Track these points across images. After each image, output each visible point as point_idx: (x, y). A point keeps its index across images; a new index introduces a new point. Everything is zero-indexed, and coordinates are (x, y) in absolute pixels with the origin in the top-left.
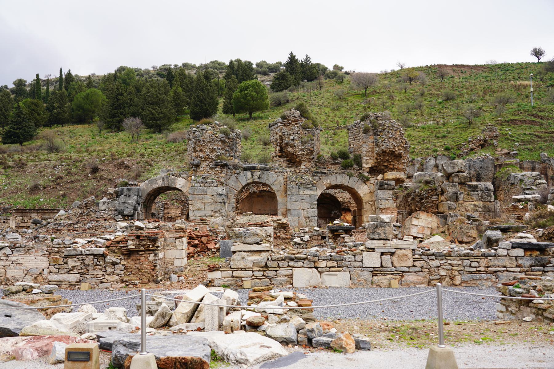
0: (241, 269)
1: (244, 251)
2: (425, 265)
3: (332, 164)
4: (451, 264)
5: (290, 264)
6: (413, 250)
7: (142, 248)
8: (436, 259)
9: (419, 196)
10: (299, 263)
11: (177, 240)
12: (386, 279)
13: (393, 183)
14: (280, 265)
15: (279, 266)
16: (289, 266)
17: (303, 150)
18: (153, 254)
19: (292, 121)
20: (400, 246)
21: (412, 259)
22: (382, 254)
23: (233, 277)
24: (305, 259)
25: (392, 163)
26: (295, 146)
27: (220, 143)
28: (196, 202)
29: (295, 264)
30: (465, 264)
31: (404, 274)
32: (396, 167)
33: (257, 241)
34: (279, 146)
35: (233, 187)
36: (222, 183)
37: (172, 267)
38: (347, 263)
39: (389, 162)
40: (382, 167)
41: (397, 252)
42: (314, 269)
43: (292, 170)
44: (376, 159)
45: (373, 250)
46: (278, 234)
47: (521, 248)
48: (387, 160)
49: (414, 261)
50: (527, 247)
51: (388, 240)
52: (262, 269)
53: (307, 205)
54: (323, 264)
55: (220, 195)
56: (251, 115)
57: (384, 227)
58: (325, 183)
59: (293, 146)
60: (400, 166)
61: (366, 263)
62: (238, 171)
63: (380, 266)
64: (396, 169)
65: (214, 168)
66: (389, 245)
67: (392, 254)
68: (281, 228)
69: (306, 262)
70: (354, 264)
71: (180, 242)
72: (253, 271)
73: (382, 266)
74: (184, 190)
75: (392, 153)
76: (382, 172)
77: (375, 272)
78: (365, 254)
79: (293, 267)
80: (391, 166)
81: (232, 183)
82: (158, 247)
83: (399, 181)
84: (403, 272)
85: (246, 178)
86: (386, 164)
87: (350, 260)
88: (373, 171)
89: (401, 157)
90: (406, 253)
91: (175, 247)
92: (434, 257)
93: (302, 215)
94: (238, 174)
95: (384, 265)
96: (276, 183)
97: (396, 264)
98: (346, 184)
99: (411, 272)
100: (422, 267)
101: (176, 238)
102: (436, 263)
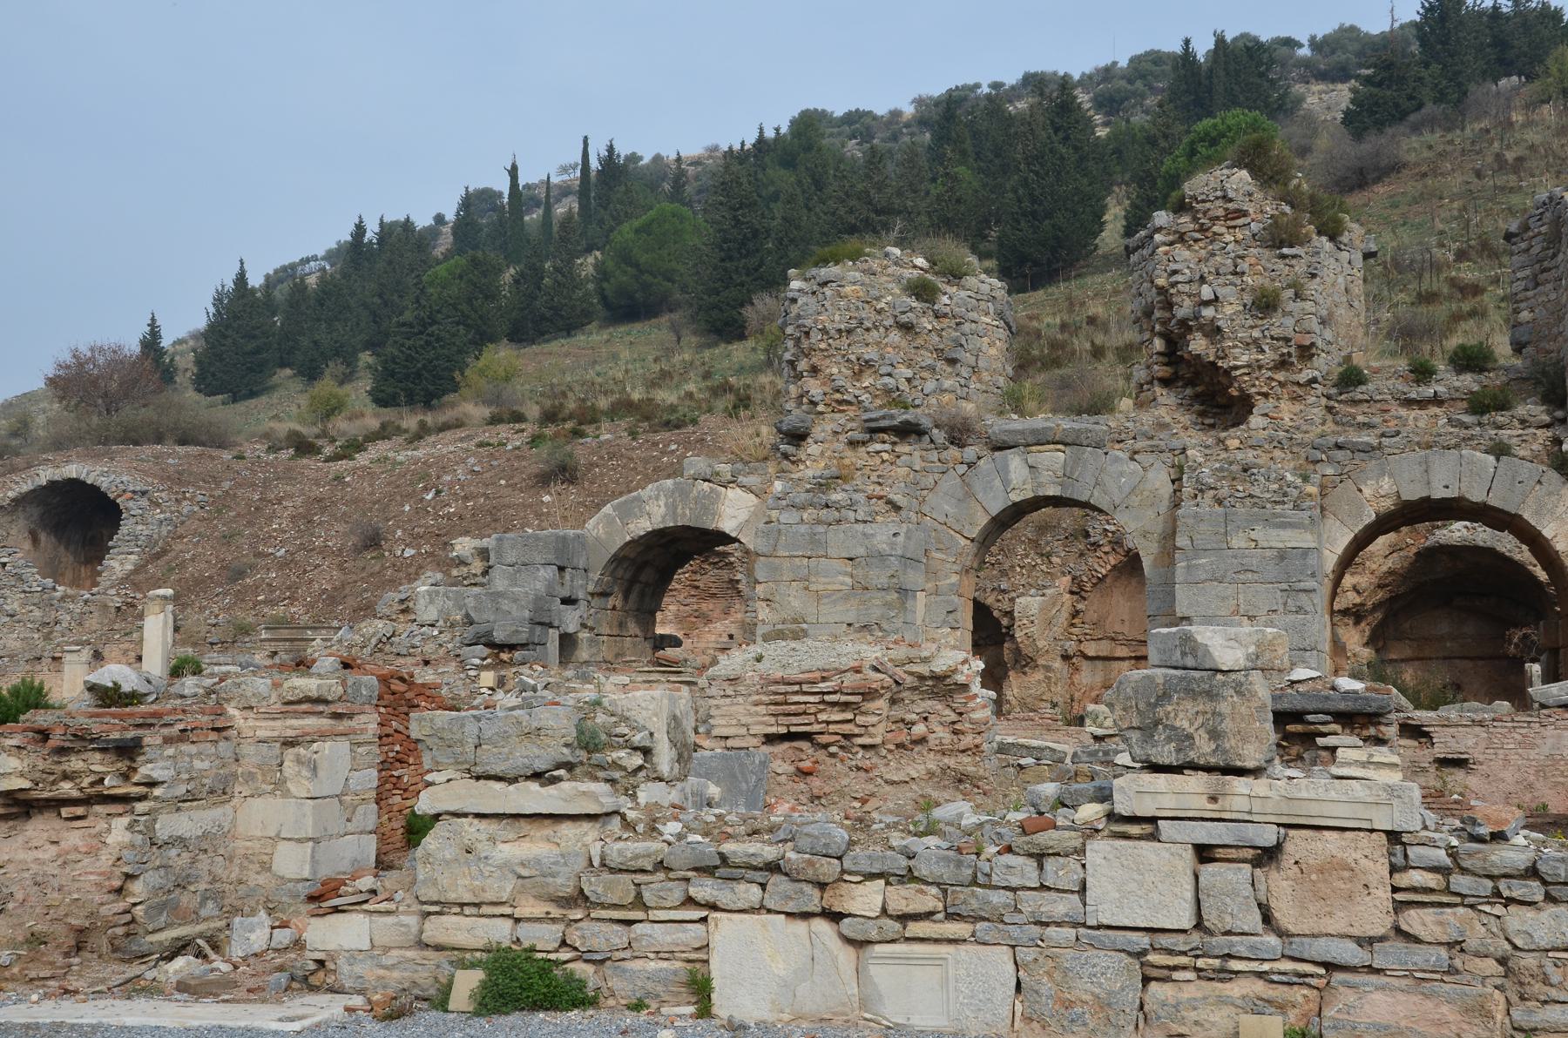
0: (462, 905)
2: (1476, 933)
3: (1408, 403)
5: (692, 891)
6: (1394, 836)
7: (67, 789)
8: (1550, 899)
10: (741, 887)
11: (290, 753)
12: (1222, 1001)
14: (647, 895)
15: (639, 902)
16: (690, 901)
17: (1256, 344)
18: (125, 820)
20: (1314, 809)
21: (1383, 895)
22: (1204, 853)
23: (423, 945)
24: (773, 867)
26: (1219, 329)
27: (895, 336)
28: (783, 588)
31: (1339, 976)
33: (540, 765)
34: (1161, 335)
35: (950, 521)
37: (261, 879)
38: (998, 898)
41: (1289, 847)
42: (822, 926)
45: (1150, 825)
46: (919, 729)
49: (1399, 907)
51: (1241, 772)
52: (556, 912)
54: (865, 899)
55: (882, 556)
57: (1211, 695)
58: (1367, 492)
59: (1213, 332)
61: (1106, 905)
62: (970, 452)
63: (1187, 921)
67: (1268, 856)
68: (934, 695)
69: (777, 882)
70: (1031, 903)
71: (299, 760)
73: (1199, 925)
78: (1099, 850)
79: (714, 907)
81: (943, 504)
84: (1330, 966)
85: (1006, 482)
87: (1015, 881)
90: (1350, 856)
91: (280, 786)
92: (1535, 890)
94: (970, 465)
95: (1211, 919)
96: (1135, 500)
97: (1285, 915)
99: (1378, 971)
100: (1455, 945)
101: (289, 743)
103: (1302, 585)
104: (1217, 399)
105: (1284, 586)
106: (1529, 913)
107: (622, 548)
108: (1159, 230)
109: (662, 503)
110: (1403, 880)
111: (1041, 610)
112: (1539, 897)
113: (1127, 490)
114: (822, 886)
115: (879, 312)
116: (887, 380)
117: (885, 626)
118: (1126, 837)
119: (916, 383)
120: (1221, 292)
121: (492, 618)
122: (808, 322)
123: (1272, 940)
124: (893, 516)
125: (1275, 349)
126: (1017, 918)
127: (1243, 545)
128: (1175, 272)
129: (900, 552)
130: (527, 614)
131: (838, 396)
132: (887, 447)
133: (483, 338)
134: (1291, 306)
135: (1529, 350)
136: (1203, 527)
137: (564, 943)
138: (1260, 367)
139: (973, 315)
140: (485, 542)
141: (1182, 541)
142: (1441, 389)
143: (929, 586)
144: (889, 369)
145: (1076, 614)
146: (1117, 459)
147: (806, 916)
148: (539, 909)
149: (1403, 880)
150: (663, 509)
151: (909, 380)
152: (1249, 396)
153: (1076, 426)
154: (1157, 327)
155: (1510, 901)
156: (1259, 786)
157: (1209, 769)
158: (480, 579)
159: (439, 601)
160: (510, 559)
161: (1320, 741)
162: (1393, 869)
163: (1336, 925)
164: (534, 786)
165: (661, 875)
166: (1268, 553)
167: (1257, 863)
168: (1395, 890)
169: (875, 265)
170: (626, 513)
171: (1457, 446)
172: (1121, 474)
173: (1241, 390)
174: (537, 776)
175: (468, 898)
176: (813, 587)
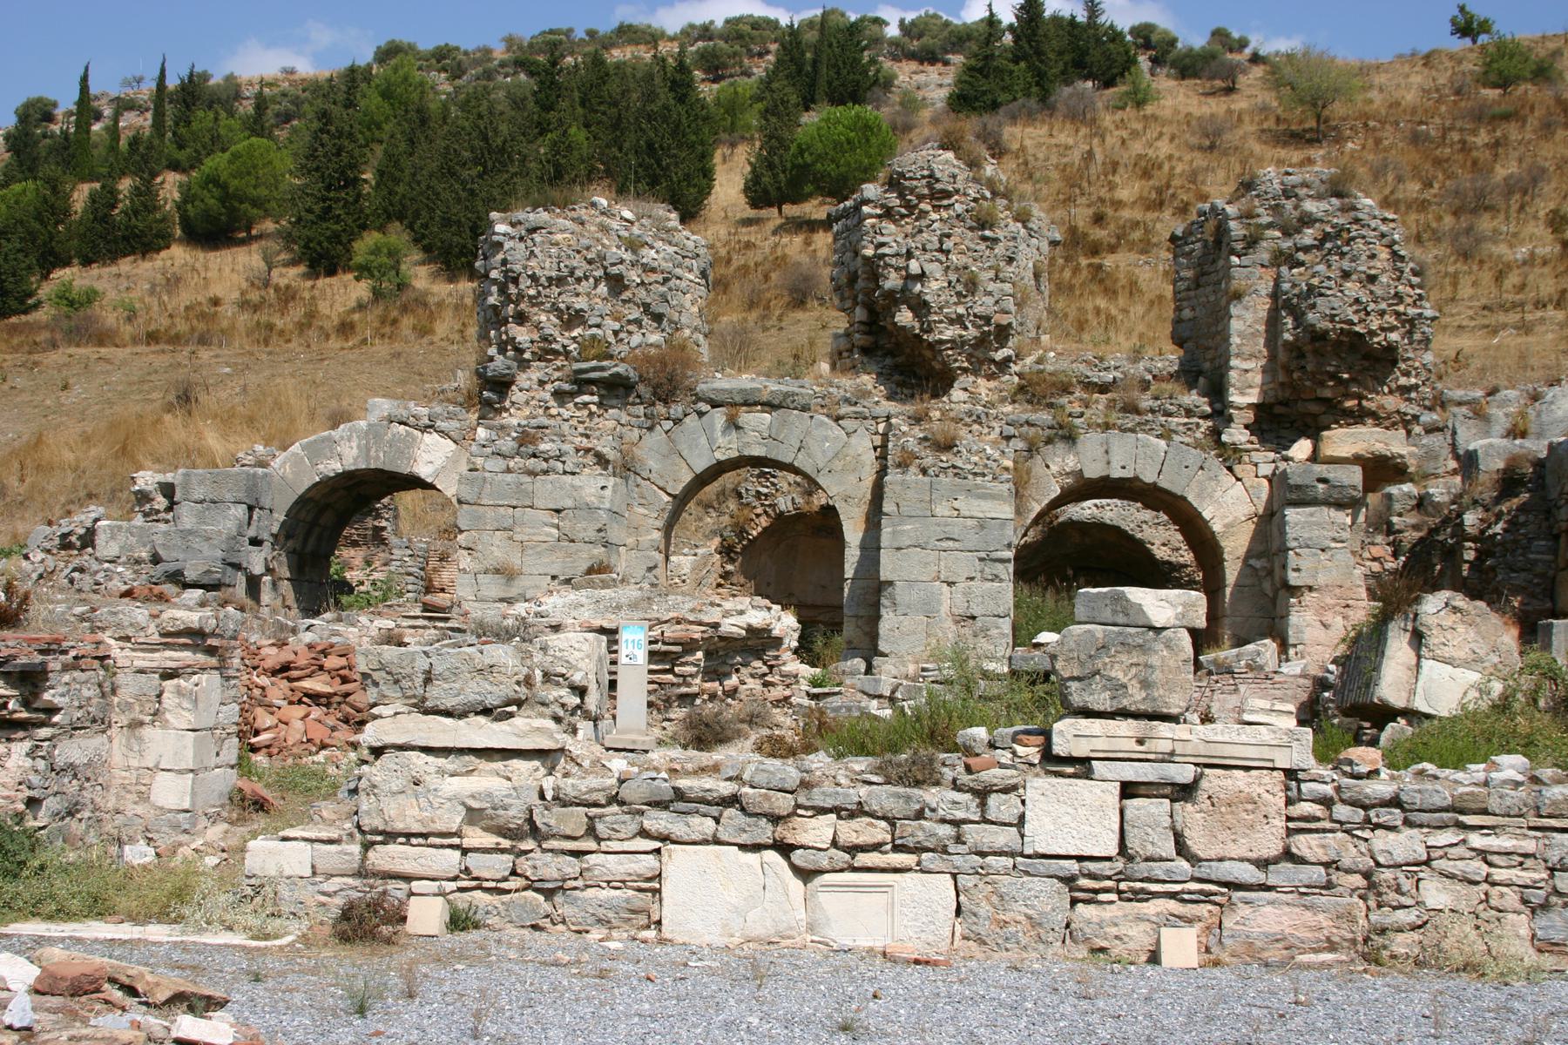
0: (409, 836)
1: (427, 750)
2: (1351, 854)
4: (1483, 854)
5: (647, 824)
6: (1290, 774)
8: (1408, 823)
10: (695, 820)
12: (1139, 919)
13: (1355, 476)
15: (591, 832)
16: (644, 833)
17: (959, 320)
18: (27, 745)
19: (921, 198)
21: (1280, 823)
22: (1129, 790)
26: (926, 303)
28: (486, 537)
29: (677, 828)
33: (491, 701)
36: (602, 460)
37: (140, 810)
39: (1341, 382)
40: (1314, 408)
41: (1204, 784)
42: (771, 856)
43: (909, 408)
45: (1082, 766)
48: (1333, 376)
49: (1290, 832)
52: (506, 843)
53: (963, 564)
54: (816, 831)
58: (1054, 468)
59: (920, 307)
60: (1391, 402)
63: (1113, 850)
65: (572, 395)
66: (1165, 746)
67: (1184, 792)
71: (179, 692)
72: (465, 852)
74: (450, 488)
76: (1313, 431)
77: (1080, 881)
79: (665, 838)
80: (1349, 404)
82: (52, 710)
83: (1381, 470)
86: (1328, 394)
87: (960, 815)
89: (1394, 362)
92: (1395, 817)
93: (944, 609)
94: (677, 421)
95: (1133, 843)
96: (838, 465)
97: (1196, 844)
98: (1149, 477)
102: (1403, 844)
105: (983, 555)
106: (1392, 836)
107: (309, 490)
108: (867, 202)
109: (354, 444)
111: (693, 569)
112: (1399, 823)
113: (830, 454)
115: (590, 262)
116: (594, 331)
119: (622, 335)
120: (928, 268)
121: (181, 557)
122: (518, 268)
123: (1185, 865)
124: (598, 469)
125: (978, 327)
126: (961, 848)
127: (947, 513)
128: (883, 245)
129: (607, 505)
130: (219, 554)
134: (991, 287)
135: (1189, 345)
136: (910, 494)
137: (514, 873)
139: (678, 271)
140: (169, 477)
141: (888, 507)
144: (599, 320)
146: (822, 424)
147: (757, 848)
148: (490, 840)
150: (355, 451)
151: (616, 333)
152: (951, 370)
153: (784, 388)
154: (860, 297)
155: (1378, 826)
156: (1179, 731)
157: (1136, 716)
158: (162, 516)
159: (122, 537)
160: (198, 496)
162: (1289, 802)
165: (615, 808)
166: (969, 522)
168: (1289, 819)
169: (582, 213)
170: (314, 452)
171: (1132, 430)
172: (826, 439)
173: (944, 363)
174: (486, 712)
175: (416, 828)
176: (517, 537)
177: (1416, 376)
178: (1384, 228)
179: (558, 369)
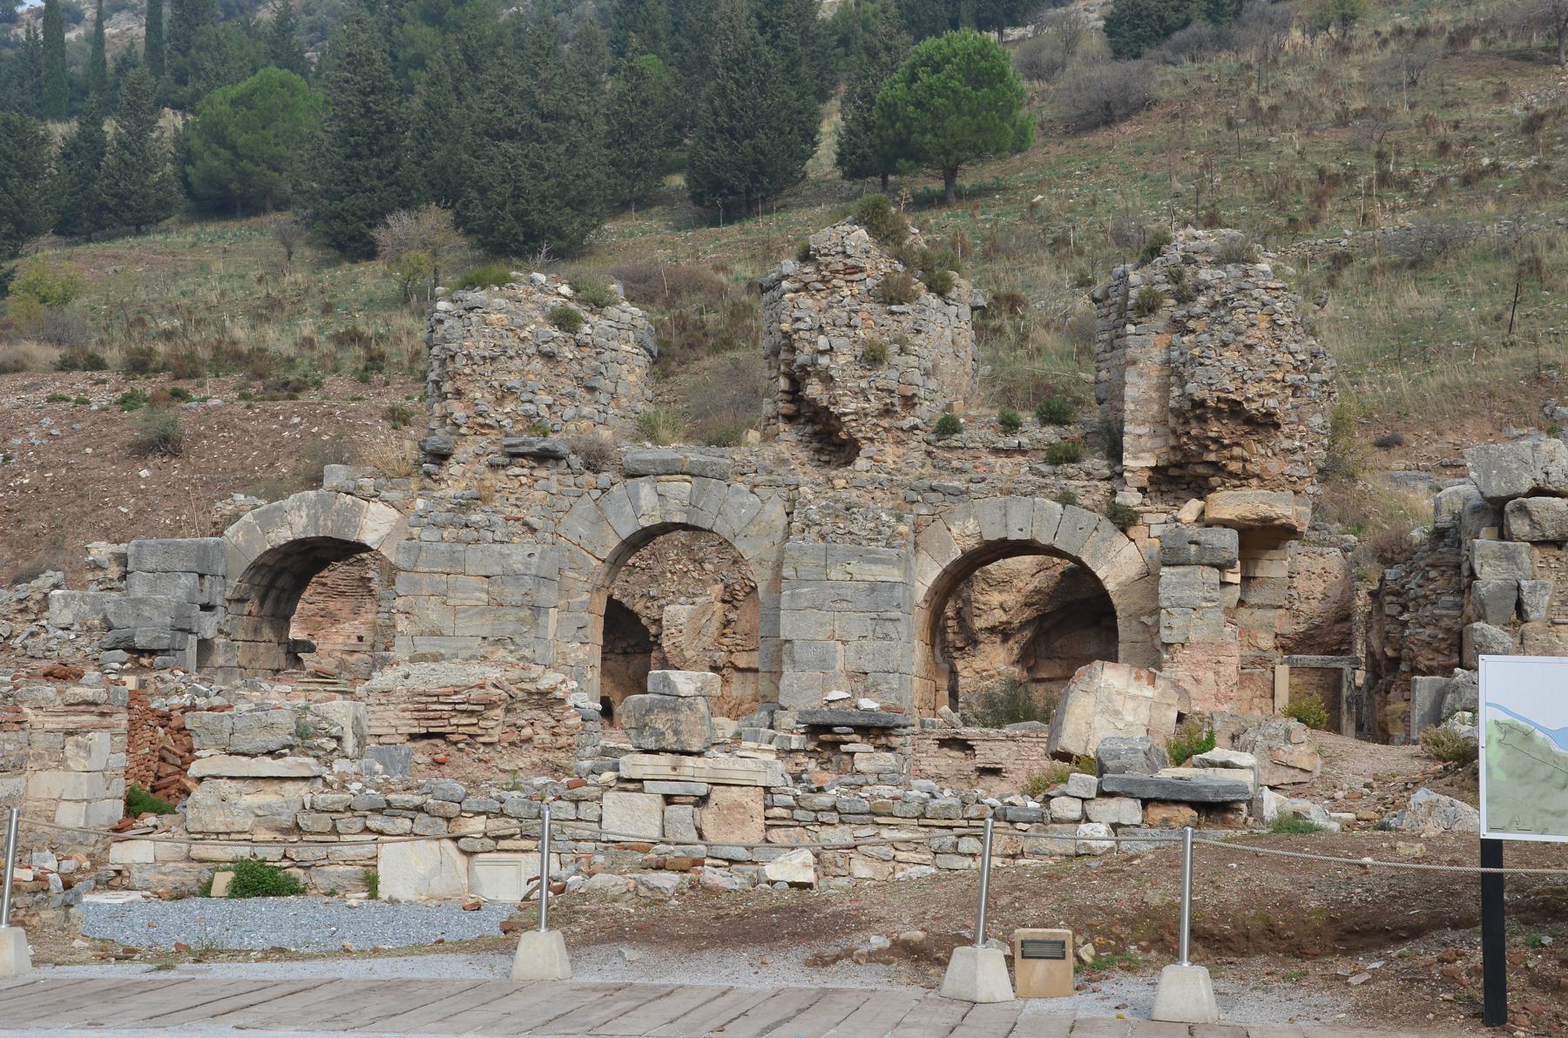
3: (997, 451)
5: (368, 823)
6: (767, 789)
8: (842, 822)
9: (1397, 594)
10: (399, 821)
14: (340, 827)
15: (334, 830)
16: (367, 830)
20: (727, 774)
21: (760, 821)
22: (669, 799)
23: (189, 859)
24: (419, 809)
25: (1237, 451)
26: (832, 378)
27: (537, 364)
28: (421, 601)
30: (935, 844)
32: (1257, 470)
33: (272, 747)
34: (786, 375)
35: (583, 542)
39: (1225, 447)
40: (1201, 470)
41: (713, 796)
42: (449, 844)
44: (1174, 432)
46: (527, 732)
47: (1130, 795)
48: (1216, 441)
50: (1151, 793)
51: (690, 754)
52: (280, 837)
54: (477, 825)
55: (517, 576)
56: (950, 174)
57: (675, 710)
58: (955, 531)
59: (828, 380)
60: (1275, 466)
62: (604, 478)
64: (1258, 476)
67: (702, 801)
68: (539, 706)
71: (77, 745)
75: (1234, 410)
76: (1201, 489)
78: (610, 798)
79: (381, 833)
80: (1234, 466)
81: (577, 526)
85: (636, 508)
86: (1212, 457)
87: (562, 816)
88: (1177, 479)
90: (744, 800)
91: (62, 763)
92: (834, 817)
96: (753, 530)
101: (69, 733)
103: (888, 615)
104: (831, 442)
105: (874, 615)
106: (830, 830)
107: (261, 557)
108: (786, 277)
109: (304, 514)
110: (770, 813)
111: (691, 618)
112: (836, 821)
113: (746, 520)
114: (449, 819)
115: (523, 340)
116: (528, 406)
117: (517, 640)
118: (626, 790)
119: (556, 409)
120: (836, 342)
121: (132, 624)
122: (454, 346)
123: (702, 848)
124: (529, 537)
125: (879, 399)
126: (563, 837)
127: (840, 577)
128: (798, 319)
129: (534, 572)
130: (168, 620)
131: (480, 420)
132: (526, 471)
133: (23, 231)
134: (896, 360)
135: (1105, 405)
136: (806, 559)
137: (285, 856)
138: (866, 415)
139: (614, 344)
140: (122, 547)
141: (787, 572)
142: (1024, 440)
143: (562, 602)
144: (530, 396)
145: (727, 623)
146: (738, 491)
148: (269, 836)
149: (770, 813)
150: (305, 520)
151: (549, 406)
152: (856, 440)
153: (702, 459)
154: (782, 368)
155: (823, 823)
157: (673, 752)
158: (116, 584)
159: (75, 606)
160: (150, 565)
161: (843, 748)
162: (766, 807)
163: (734, 839)
164: (268, 759)
165: (349, 814)
166: (861, 585)
167: (696, 805)
169: (520, 292)
170: (266, 521)
171: (1032, 493)
172: (742, 505)
173: (849, 434)
174: (270, 753)
176: (451, 602)
177: (1302, 438)
178: (1266, 298)
179: (493, 443)
